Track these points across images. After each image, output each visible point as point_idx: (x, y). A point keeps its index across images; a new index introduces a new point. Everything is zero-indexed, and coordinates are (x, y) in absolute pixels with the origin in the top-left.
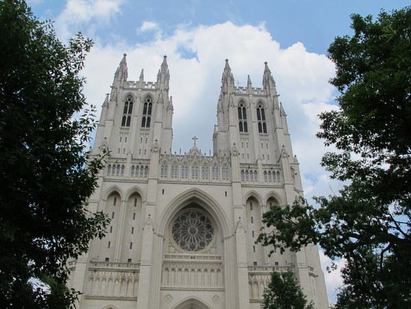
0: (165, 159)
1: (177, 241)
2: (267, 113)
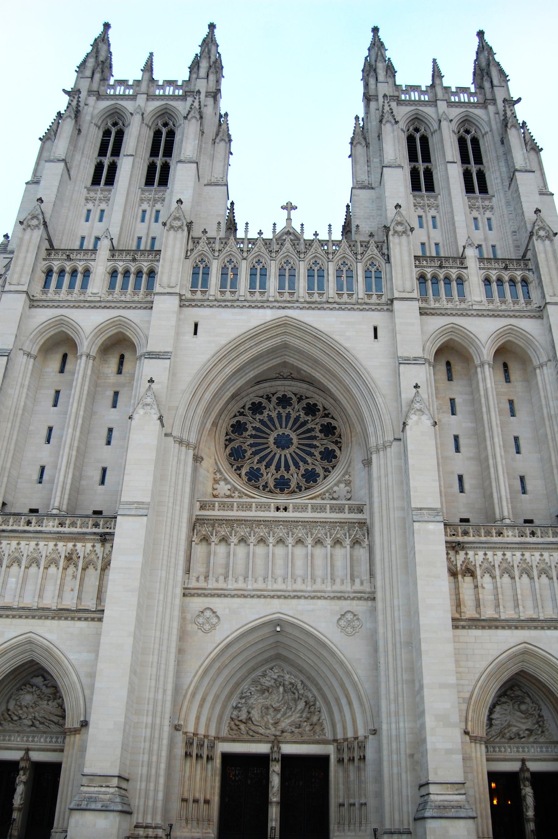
0: (202, 246)
1: (239, 468)
2: (487, 146)
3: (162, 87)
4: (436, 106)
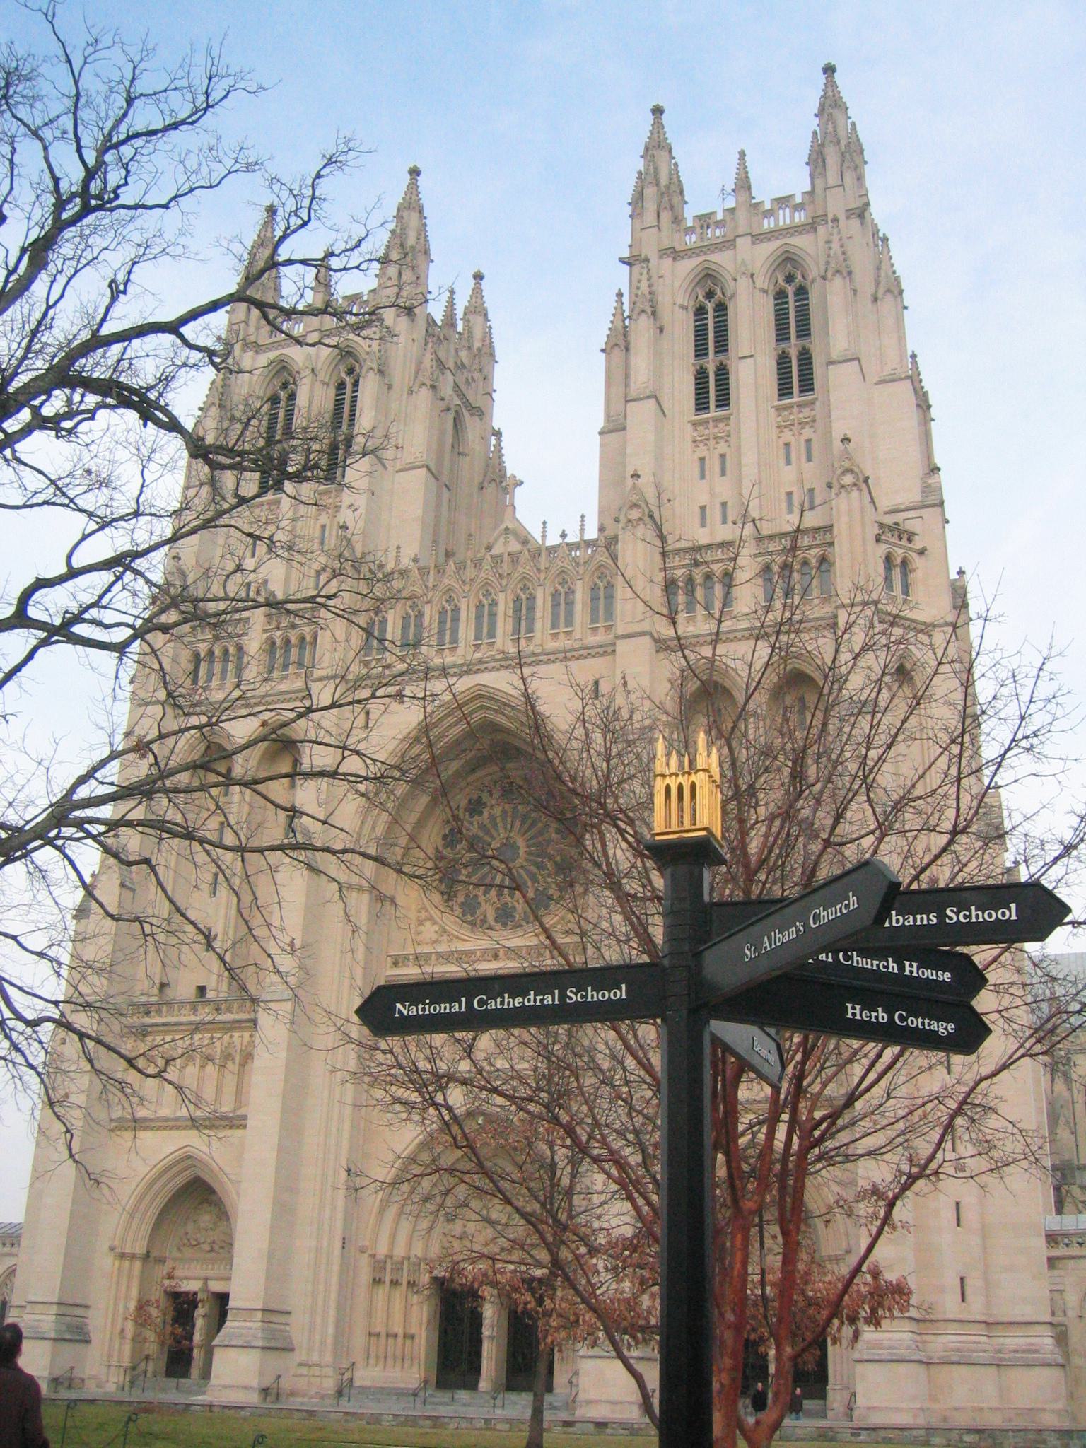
3: (769, 214)
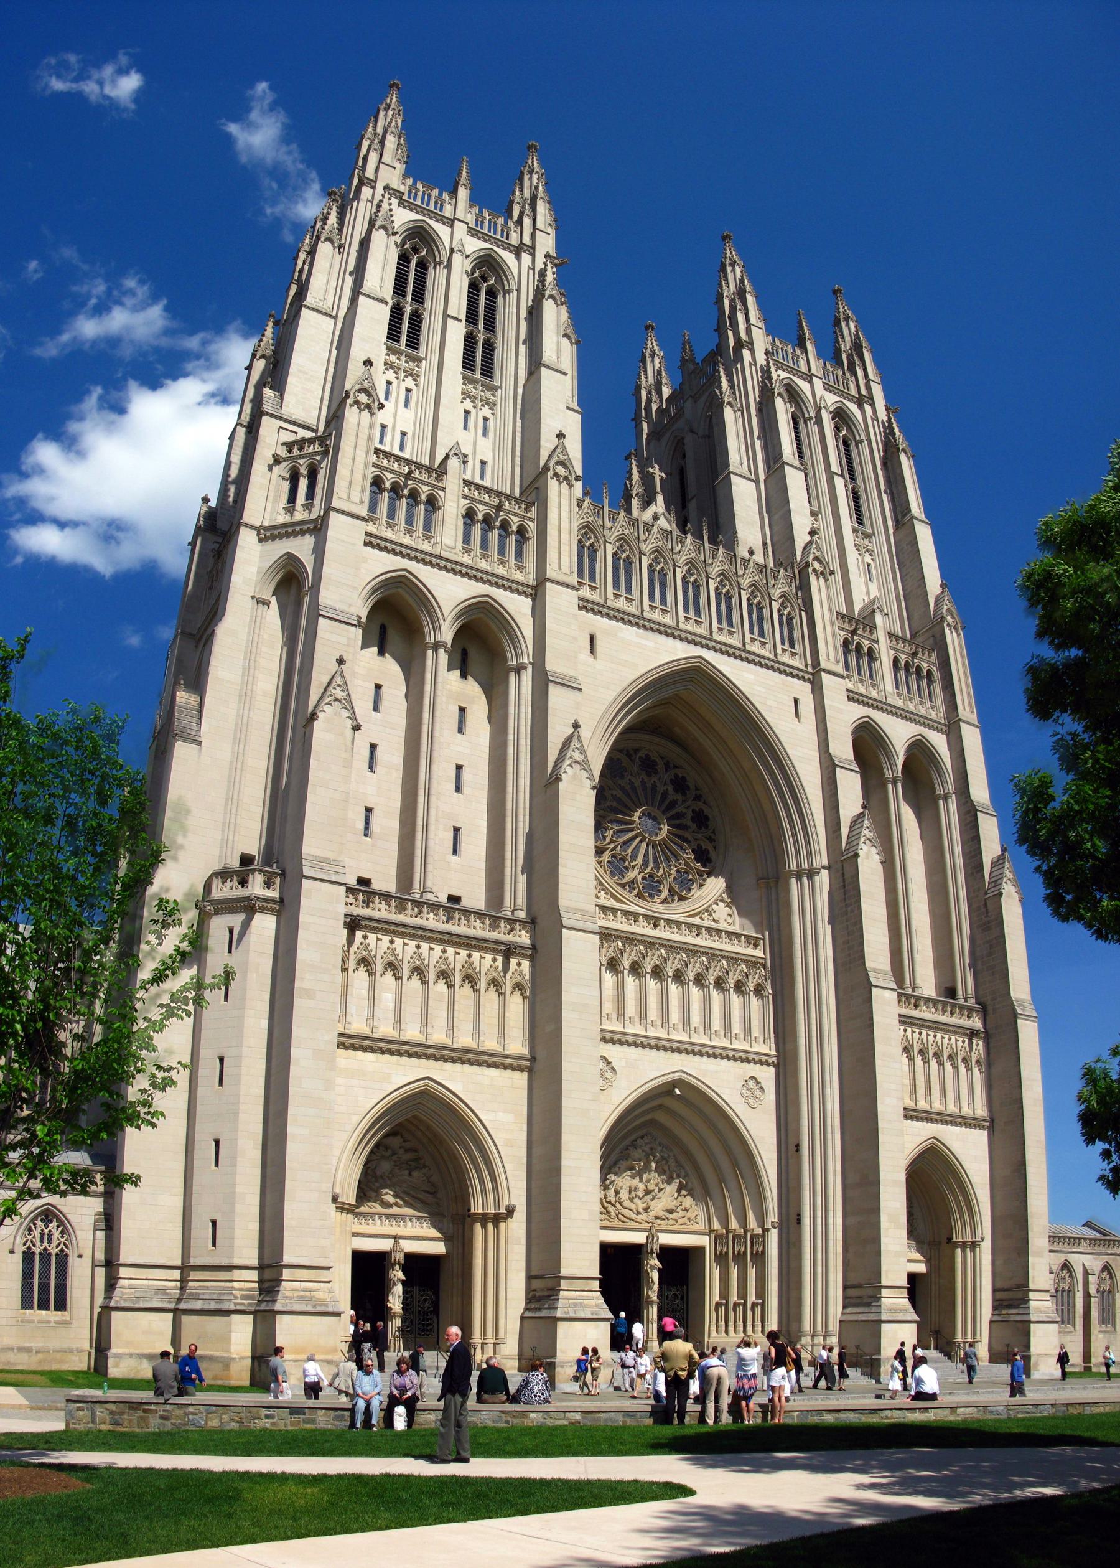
4: (452, 226)
